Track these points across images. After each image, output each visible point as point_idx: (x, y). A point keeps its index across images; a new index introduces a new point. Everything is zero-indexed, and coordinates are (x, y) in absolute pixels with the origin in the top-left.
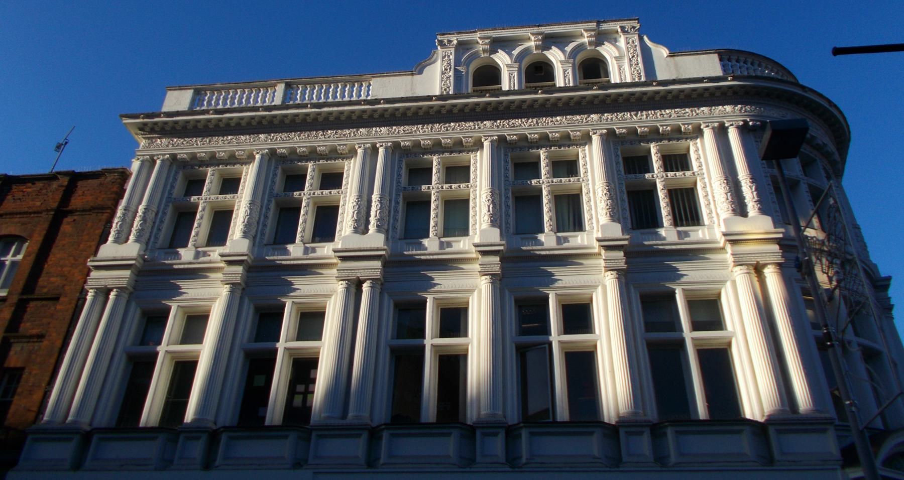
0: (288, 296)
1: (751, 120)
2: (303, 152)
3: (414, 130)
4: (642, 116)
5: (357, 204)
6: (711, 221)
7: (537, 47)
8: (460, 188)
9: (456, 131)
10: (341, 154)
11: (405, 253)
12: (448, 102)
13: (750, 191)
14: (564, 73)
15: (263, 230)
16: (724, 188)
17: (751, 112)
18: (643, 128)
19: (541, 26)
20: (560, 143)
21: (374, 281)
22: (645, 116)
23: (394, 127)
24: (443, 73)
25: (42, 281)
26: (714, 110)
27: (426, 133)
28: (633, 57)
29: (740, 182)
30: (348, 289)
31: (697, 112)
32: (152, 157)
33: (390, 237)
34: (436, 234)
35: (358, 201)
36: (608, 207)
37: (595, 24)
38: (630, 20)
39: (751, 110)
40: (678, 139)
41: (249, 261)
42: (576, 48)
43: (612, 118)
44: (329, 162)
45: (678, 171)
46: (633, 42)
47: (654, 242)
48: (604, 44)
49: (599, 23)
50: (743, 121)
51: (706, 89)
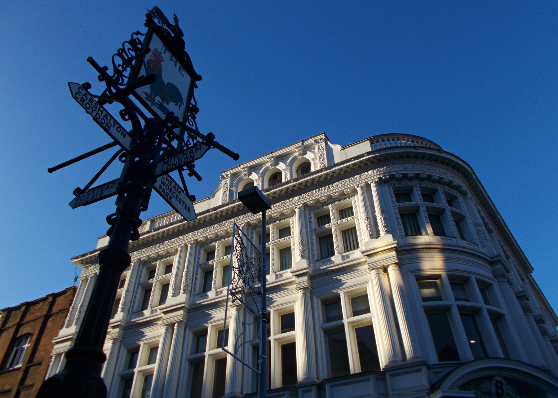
0: (141, 340)
1: (383, 176)
2: (153, 256)
3: (205, 230)
4: (322, 190)
5: (175, 279)
6: (362, 245)
7: (271, 165)
8: (228, 258)
9: (226, 226)
10: (172, 253)
11: (197, 302)
12: (218, 211)
13: (381, 221)
14: (285, 175)
15: (133, 305)
16: (366, 223)
17: (383, 171)
18: (322, 198)
19: (273, 152)
20: (280, 218)
21: (180, 322)
22: (323, 190)
23: (196, 231)
24: (223, 194)
25: (37, 355)
26: (362, 175)
27: (211, 230)
28: (321, 156)
29: (376, 217)
30: (166, 330)
31: (353, 179)
32: (86, 277)
33: (192, 295)
34: (215, 287)
35: (176, 278)
36: (300, 251)
37: (301, 142)
38: (320, 135)
39: (383, 170)
40: (344, 199)
41: (123, 324)
42: (293, 160)
43: (305, 196)
44: (167, 259)
45: (349, 217)
46: (322, 147)
47: (326, 266)
48: (307, 153)
49: (303, 141)
50: (378, 178)
51: (354, 164)
